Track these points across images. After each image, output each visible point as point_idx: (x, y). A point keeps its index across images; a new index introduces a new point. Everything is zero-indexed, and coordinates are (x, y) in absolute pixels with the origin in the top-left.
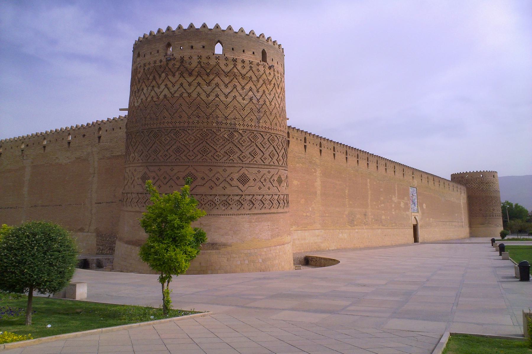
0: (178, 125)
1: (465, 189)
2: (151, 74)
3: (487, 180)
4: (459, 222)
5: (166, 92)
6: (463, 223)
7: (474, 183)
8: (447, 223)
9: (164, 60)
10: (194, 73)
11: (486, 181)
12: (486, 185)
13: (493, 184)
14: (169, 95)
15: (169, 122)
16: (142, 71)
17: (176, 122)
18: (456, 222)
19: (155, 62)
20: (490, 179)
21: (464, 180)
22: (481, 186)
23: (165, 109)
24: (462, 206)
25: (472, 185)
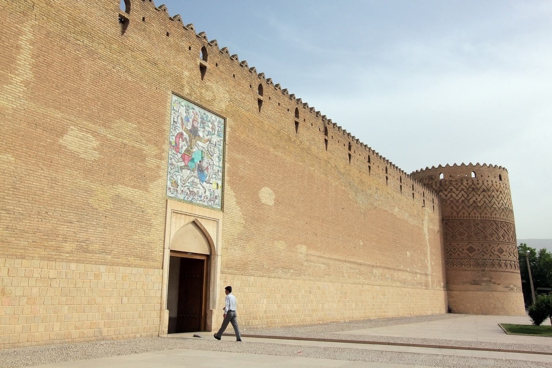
1: (436, 201)
3: (486, 184)
4: (416, 273)
6: (430, 279)
7: (457, 190)
8: (375, 271)
11: (483, 187)
12: (484, 196)
13: (499, 193)
18: (407, 271)
20: (492, 181)
21: (434, 183)
22: (471, 195)
24: (427, 237)
25: (453, 194)
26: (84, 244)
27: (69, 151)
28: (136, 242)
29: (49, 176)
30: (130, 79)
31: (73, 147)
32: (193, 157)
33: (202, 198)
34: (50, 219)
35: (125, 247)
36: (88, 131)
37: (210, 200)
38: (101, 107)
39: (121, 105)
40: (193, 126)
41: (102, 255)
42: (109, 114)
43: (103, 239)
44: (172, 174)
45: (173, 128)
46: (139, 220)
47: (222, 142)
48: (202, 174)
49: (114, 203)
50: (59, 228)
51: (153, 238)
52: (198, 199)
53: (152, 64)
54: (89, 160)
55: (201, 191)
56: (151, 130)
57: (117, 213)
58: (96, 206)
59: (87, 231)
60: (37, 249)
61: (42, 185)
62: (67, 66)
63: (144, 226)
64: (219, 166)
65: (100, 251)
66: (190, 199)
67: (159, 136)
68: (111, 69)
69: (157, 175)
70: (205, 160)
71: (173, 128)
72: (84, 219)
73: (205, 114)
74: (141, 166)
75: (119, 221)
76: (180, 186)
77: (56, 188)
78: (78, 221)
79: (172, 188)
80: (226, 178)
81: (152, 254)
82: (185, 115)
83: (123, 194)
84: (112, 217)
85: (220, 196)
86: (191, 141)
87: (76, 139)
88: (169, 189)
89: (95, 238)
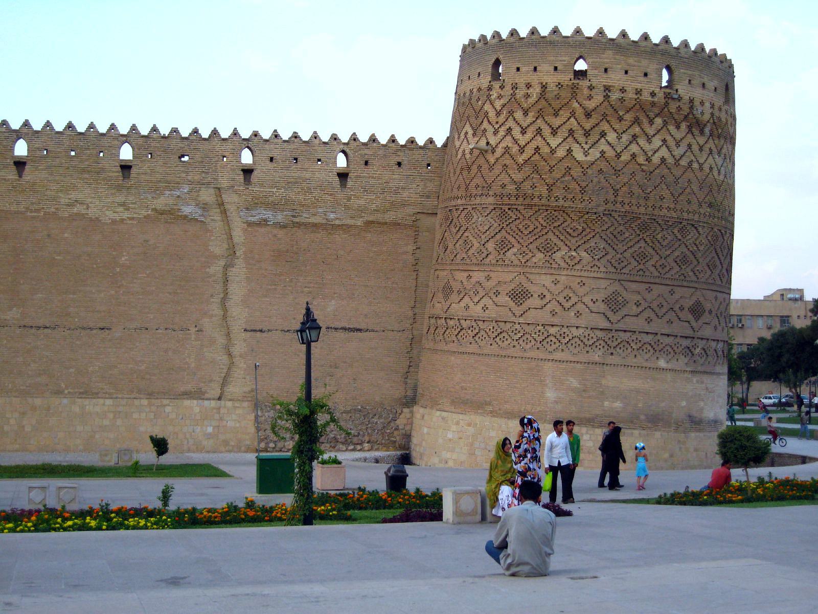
0: (685, 215)
2: (628, 111)
5: (664, 152)
9: (660, 95)
10: (707, 130)
14: (670, 160)
15: (670, 208)
16: (598, 98)
17: (682, 211)
19: (638, 92)
23: (663, 183)
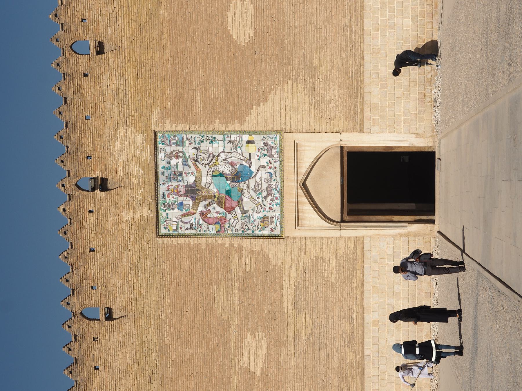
26: (346, 340)
27: (264, 365)
28: (338, 278)
29: (291, 381)
30: (168, 301)
31: (260, 360)
32: (224, 192)
33: (272, 171)
34: (328, 376)
35: (344, 292)
36: (239, 346)
37: (271, 156)
38: (211, 333)
39: (200, 309)
40: (186, 195)
41: (355, 319)
42: (214, 323)
43: (339, 319)
44: (255, 228)
45: (199, 229)
46: (314, 276)
47: (189, 136)
48: (243, 174)
49: (302, 310)
50: (335, 367)
51: (331, 254)
52: (274, 180)
53: (138, 271)
54: (268, 343)
55: (263, 174)
56: (213, 266)
57: (312, 305)
58: (309, 331)
59: (334, 337)
60: (355, 386)
61: (300, 387)
62: (186, 374)
63: (319, 268)
64: (223, 140)
65: (351, 321)
66: (278, 195)
67: (216, 254)
68: (168, 325)
69: (261, 254)
70: (222, 169)
71: (199, 229)
72: (323, 342)
73: (163, 173)
74: (257, 277)
75: (319, 301)
76: (265, 213)
77: (300, 374)
78: (326, 348)
79: (270, 226)
80: (235, 126)
81: (349, 254)
82: (176, 210)
83: (291, 300)
84: (316, 311)
85: (262, 136)
86: (205, 198)
87: (251, 357)
88: (272, 230)
89: (339, 328)
